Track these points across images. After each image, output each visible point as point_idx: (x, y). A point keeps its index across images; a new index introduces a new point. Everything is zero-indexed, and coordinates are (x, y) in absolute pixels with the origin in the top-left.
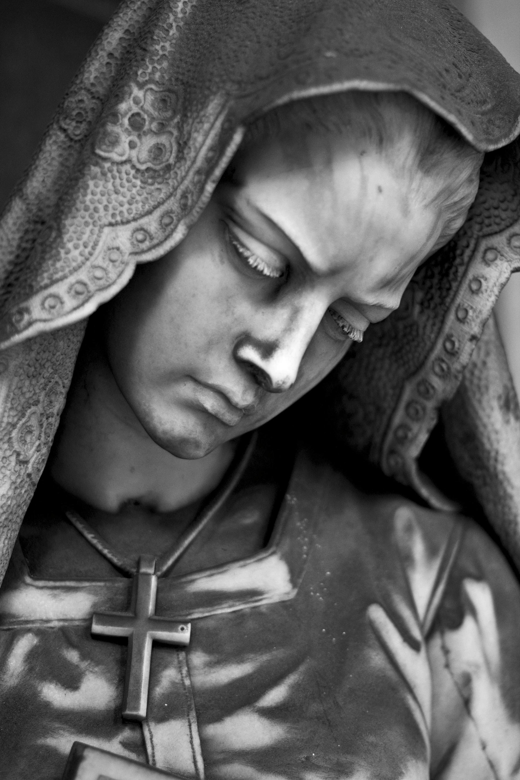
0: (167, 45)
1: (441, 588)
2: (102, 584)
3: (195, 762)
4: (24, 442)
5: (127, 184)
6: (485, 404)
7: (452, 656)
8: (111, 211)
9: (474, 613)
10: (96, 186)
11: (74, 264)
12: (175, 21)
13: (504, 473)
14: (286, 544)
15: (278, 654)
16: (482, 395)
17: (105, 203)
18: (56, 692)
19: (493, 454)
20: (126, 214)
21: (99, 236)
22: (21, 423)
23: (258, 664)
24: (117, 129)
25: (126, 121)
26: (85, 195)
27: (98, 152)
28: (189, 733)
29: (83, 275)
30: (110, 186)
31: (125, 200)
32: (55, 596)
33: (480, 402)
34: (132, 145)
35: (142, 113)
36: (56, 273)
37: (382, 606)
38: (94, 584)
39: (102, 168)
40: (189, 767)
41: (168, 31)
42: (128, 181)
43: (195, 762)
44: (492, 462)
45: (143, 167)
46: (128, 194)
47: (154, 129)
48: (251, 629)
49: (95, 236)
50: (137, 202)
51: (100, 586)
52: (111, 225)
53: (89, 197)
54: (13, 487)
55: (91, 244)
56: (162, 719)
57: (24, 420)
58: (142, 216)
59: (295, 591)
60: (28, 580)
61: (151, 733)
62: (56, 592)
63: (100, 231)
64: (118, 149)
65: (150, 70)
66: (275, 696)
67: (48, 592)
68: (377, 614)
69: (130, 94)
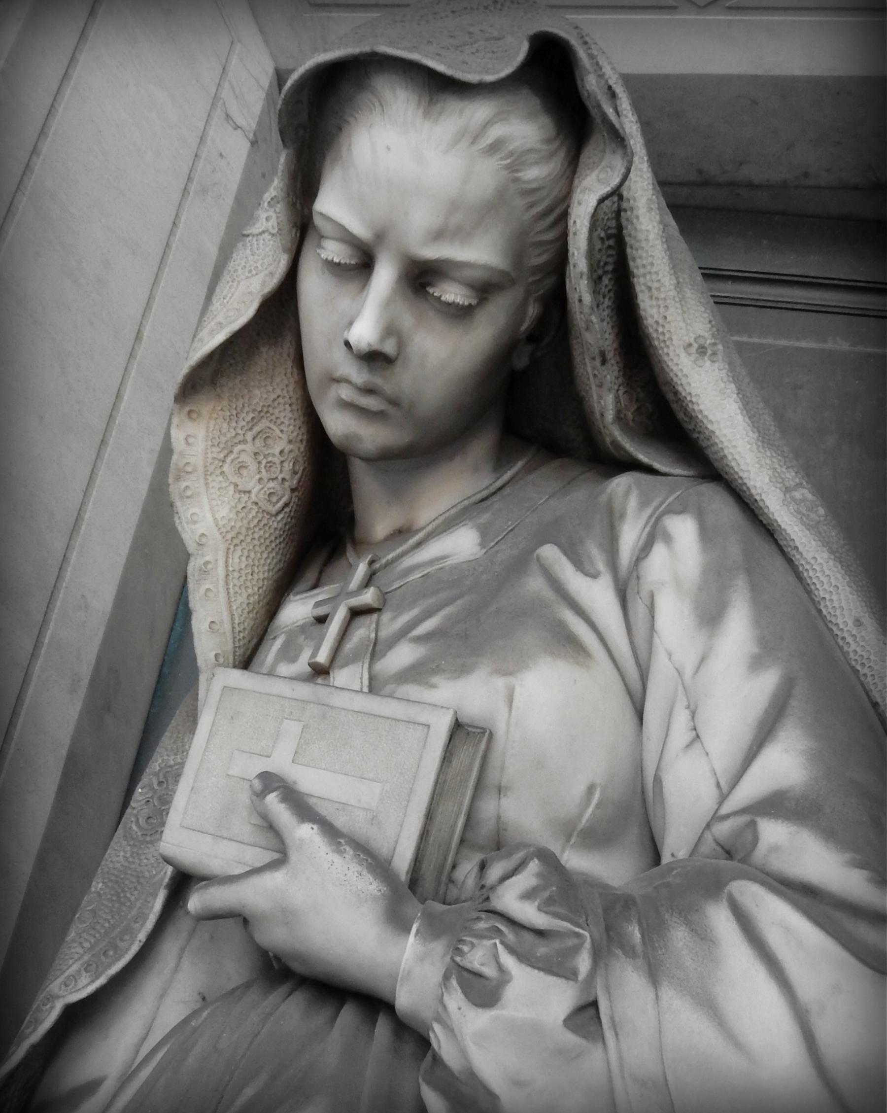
1: (648, 529)
4: (241, 475)
6: (671, 354)
7: (641, 581)
8: (247, 270)
9: (668, 539)
13: (701, 411)
14: (484, 518)
15: (444, 595)
16: (668, 347)
17: (243, 264)
19: (688, 399)
20: (260, 267)
21: (236, 289)
22: (229, 460)
25: (266, 204)
27: (245, 232)
29: (220, 318)
30: (248, 251)
33: (668, 354)
34: (267, 219)
44: (690, 405)
49: (233, 290)
52: (247, 278)
54: (234, 511)
55: (230, 295)
57: (232, 457)
59: (484, 551)
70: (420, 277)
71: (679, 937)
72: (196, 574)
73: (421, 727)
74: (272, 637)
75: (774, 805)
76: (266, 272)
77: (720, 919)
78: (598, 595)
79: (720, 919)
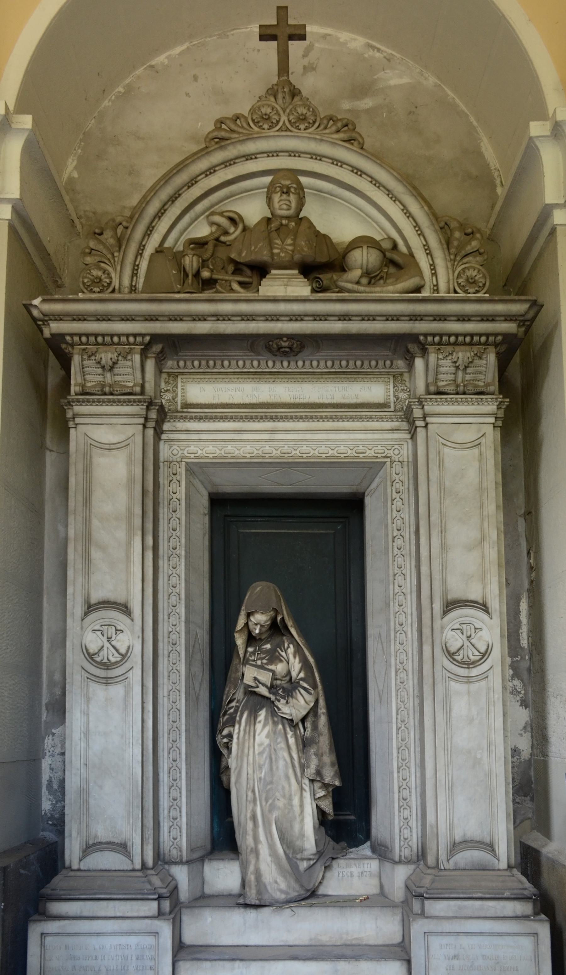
48: (267, 652)
68: (278, 649)
70: (261, 626)
71: (294, 693)
75: (301, 679)
77: (297, 691)
78: (283, 654)
79: (297, 691)
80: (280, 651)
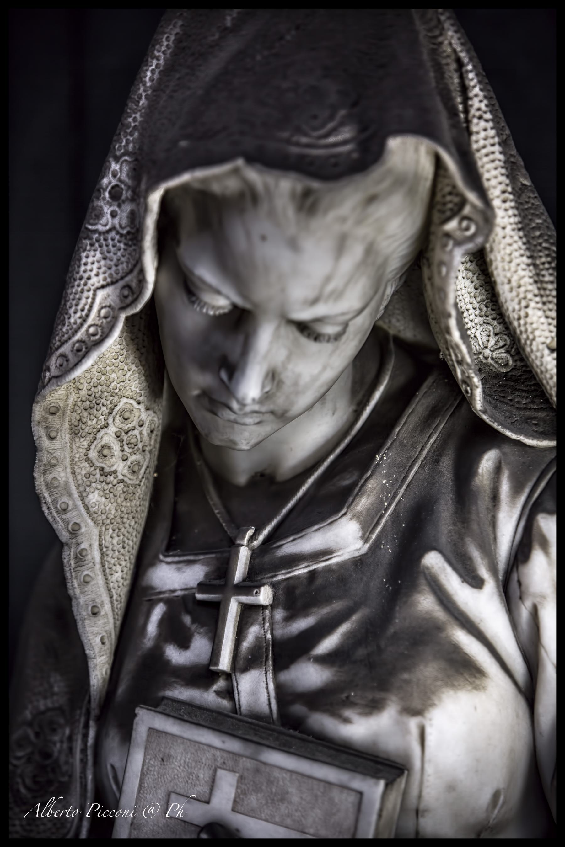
0: (138, 115)
1: (522, 524)
2: (213, 556)
3: (270, 704)
5: (113, 250)
7: (523, 588)
10: (87, 257)
11: (75, 326)
12: (145, 91)
18: (174, 651)
20: (115, 275)
23: (320, 617)
24: (101, 203)
25: (107, 195)
26: (79, 266)
28: (265, 680)
31: (112, 263)
32: (179, 569)
34: (113, 215)
35: (119, 184)
36: (63, 336)
37: (441, 552)
38: (207, 556)
39: (91, 239)
40: (266, 709)
41: (139, 102)
42: (114, 246)
43: (270, 704)
45: (124, 232)
46: (115, 258)
47: (129, 197)
50: (122, 263)
51: (211, 558)
53: (83, 268)
55: (87, 307)
56: (245, 670)
58: (128, 274)
59: (367, 546)
60: (161, 557)
61: (237, 682)
62: (180, 566)
63: (95, 295)
64: (103, 221)
65: (123, 144)
66: (329, 643)
67: (174, 566)
69: (110, 168)
72: (72, 562)
73: (354, 793)
74: (147, 599)
76: (121, 284)
80: (453, 582)
